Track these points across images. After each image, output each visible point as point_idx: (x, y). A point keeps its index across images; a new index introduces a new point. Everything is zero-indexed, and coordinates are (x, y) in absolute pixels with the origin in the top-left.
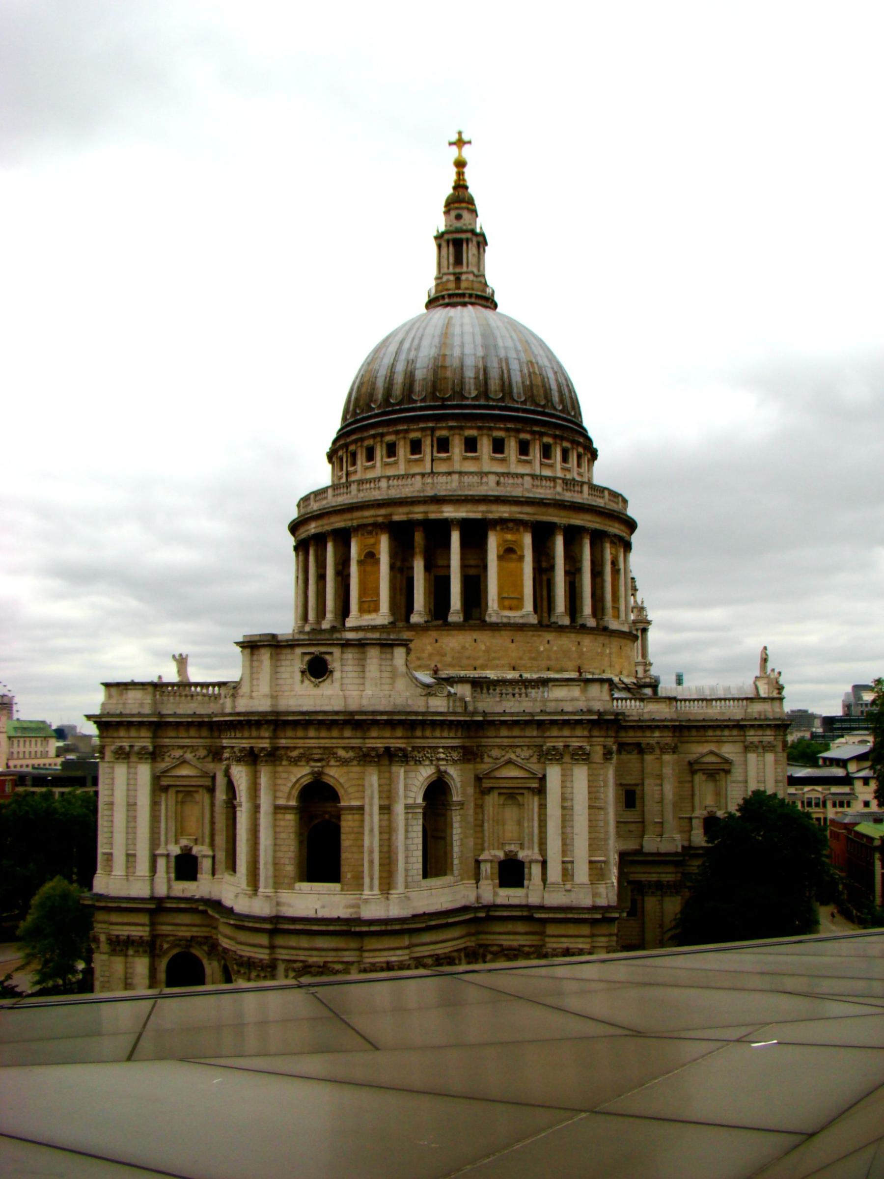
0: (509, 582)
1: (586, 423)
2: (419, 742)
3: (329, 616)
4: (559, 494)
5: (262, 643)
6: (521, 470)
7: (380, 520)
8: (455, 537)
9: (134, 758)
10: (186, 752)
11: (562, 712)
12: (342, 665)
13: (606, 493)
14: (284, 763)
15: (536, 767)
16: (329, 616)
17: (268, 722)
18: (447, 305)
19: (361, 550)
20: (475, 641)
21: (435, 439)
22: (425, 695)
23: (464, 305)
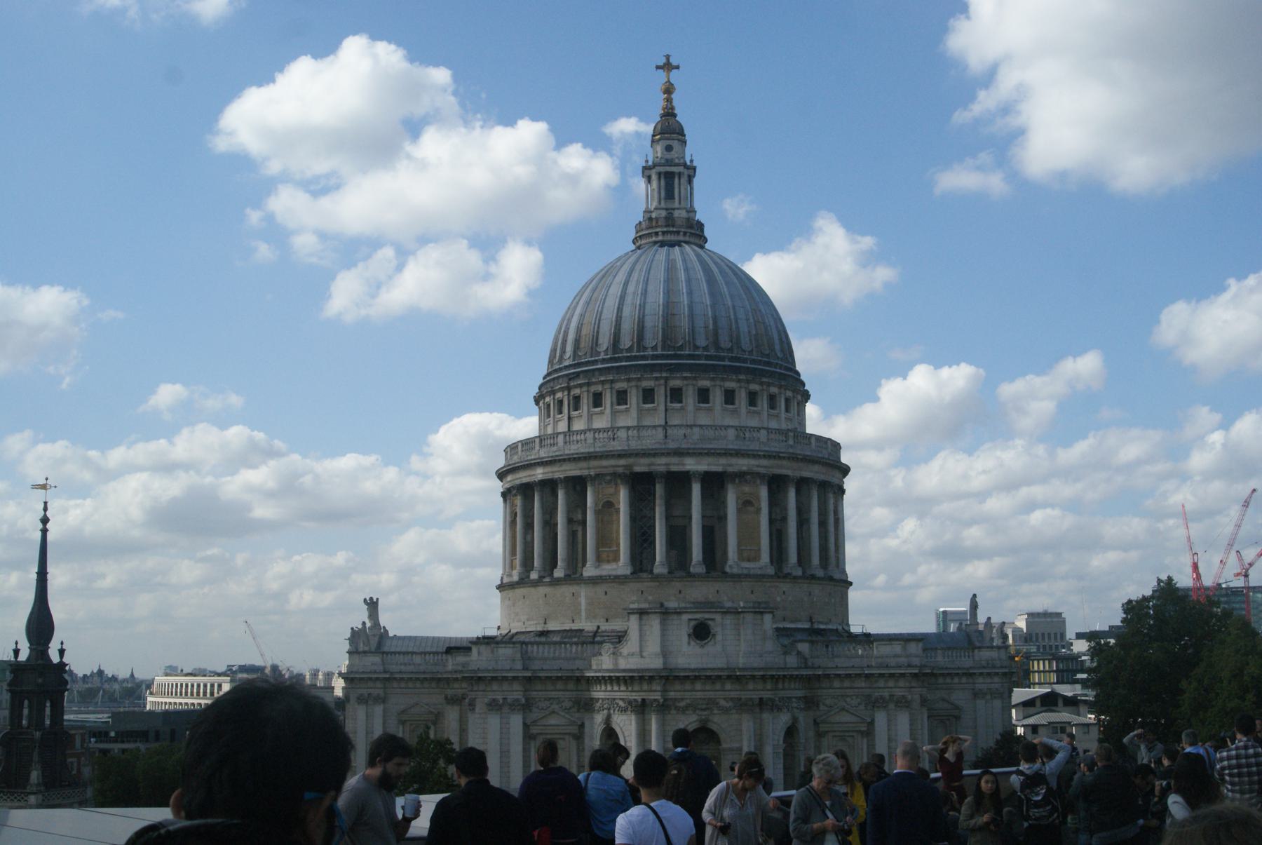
1: (799, 367)
2: (782, 694)
4: (791, 446)
6: (754, 422)
7: (620, 470)
8: (696, 489)
9: (506, 709)
10: (552, 704)
13: (829, 443)
14: (673, 712)
17: (661, 677)
18: (662, 244)
20: (718, 591)
21: (668, 389)
23: (678, 244)
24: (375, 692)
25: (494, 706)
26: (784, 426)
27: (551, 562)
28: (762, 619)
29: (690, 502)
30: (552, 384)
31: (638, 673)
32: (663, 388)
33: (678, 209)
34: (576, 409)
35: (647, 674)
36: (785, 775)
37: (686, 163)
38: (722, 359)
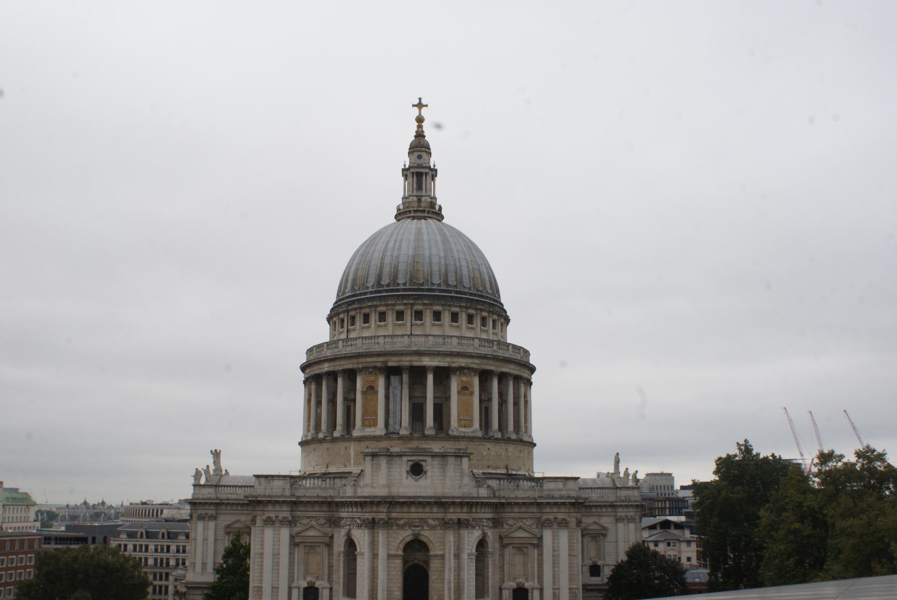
0: (466, 409)
1: (502, 301)
3: (339, 428)
4: (496, 351)
5: (381, 454)
7: (379, 365)
9: (277, 524)
10: (311, 521)
11: (553, 497)
12: (432, 468)
13: (522, 350)
14: (394, 528)
15: (536, 531)
16: (339, 427)
17: (386, 502)
18: (414, 218)
19: (364, 384)
21: (413, 311)
22: (477, 487)
23: (425, 218)
24: (210, 512)
25: (269, 522)
26: (491, 338)
27: (333, 425)
28: (461, 461)
29: (425, 386)
30: (337, 309)
31: (370, 498)
32: (409, 311)
33: (424, 196)
34: (353, 324)
35: (376, 500)
36: (477, 575)
37: (430, 167)
38: (450, 292)
